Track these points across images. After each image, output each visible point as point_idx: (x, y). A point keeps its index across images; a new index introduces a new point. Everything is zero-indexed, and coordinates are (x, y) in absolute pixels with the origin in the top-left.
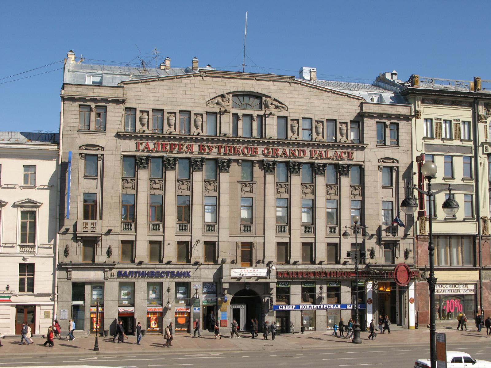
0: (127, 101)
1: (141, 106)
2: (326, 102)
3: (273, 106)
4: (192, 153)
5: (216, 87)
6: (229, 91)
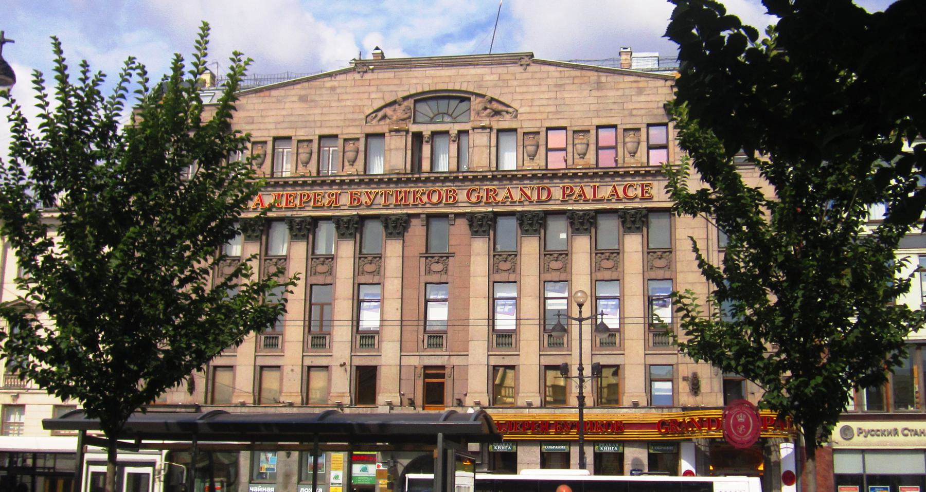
2: (595, 93)
3: (488, 111)
4: (337, 208)
5: (385, 88)
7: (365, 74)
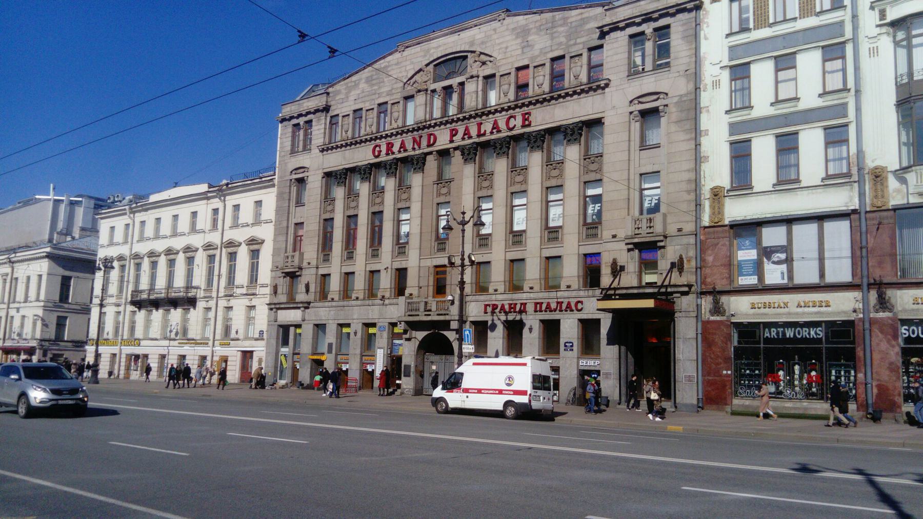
0: (332, 108)
1: (343, 110)
3: (478, 63)
6: (428, 62)
7: (404, 52)
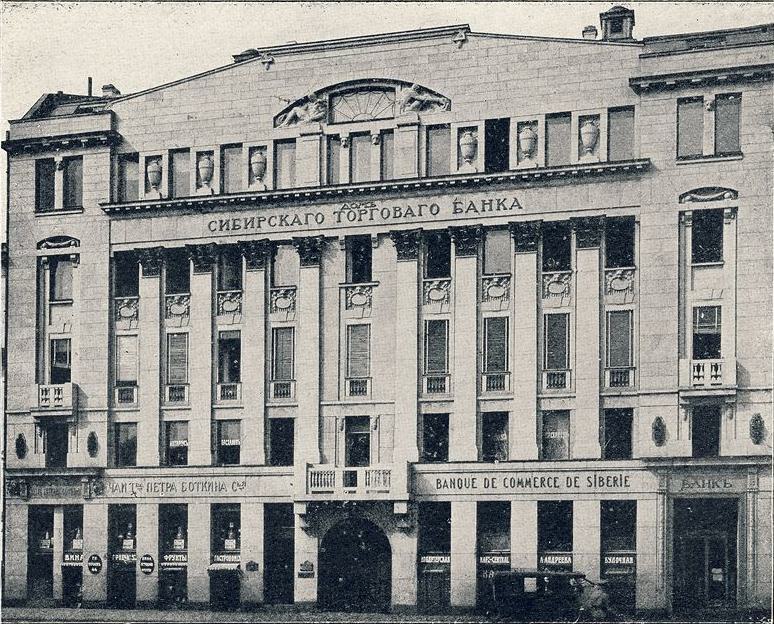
3: (416, 103)
